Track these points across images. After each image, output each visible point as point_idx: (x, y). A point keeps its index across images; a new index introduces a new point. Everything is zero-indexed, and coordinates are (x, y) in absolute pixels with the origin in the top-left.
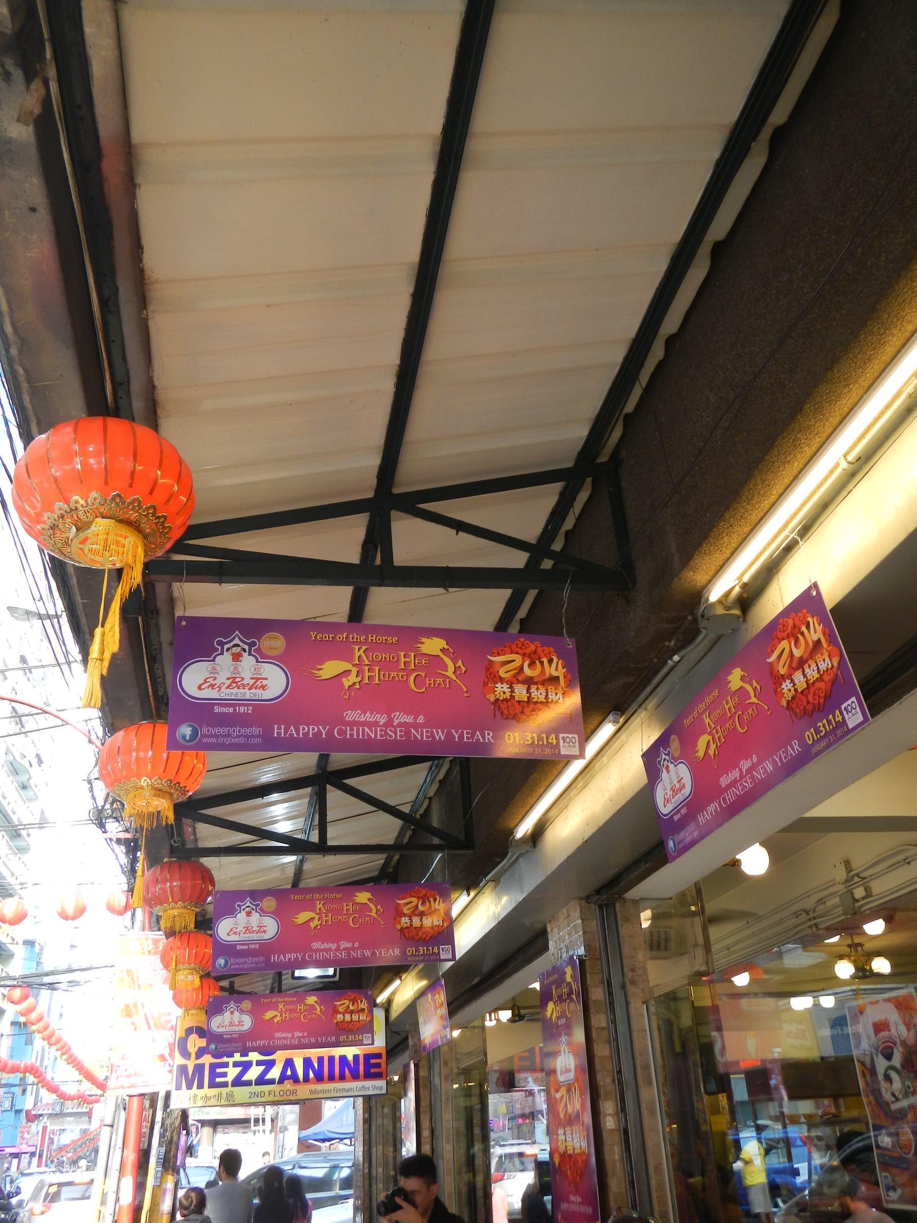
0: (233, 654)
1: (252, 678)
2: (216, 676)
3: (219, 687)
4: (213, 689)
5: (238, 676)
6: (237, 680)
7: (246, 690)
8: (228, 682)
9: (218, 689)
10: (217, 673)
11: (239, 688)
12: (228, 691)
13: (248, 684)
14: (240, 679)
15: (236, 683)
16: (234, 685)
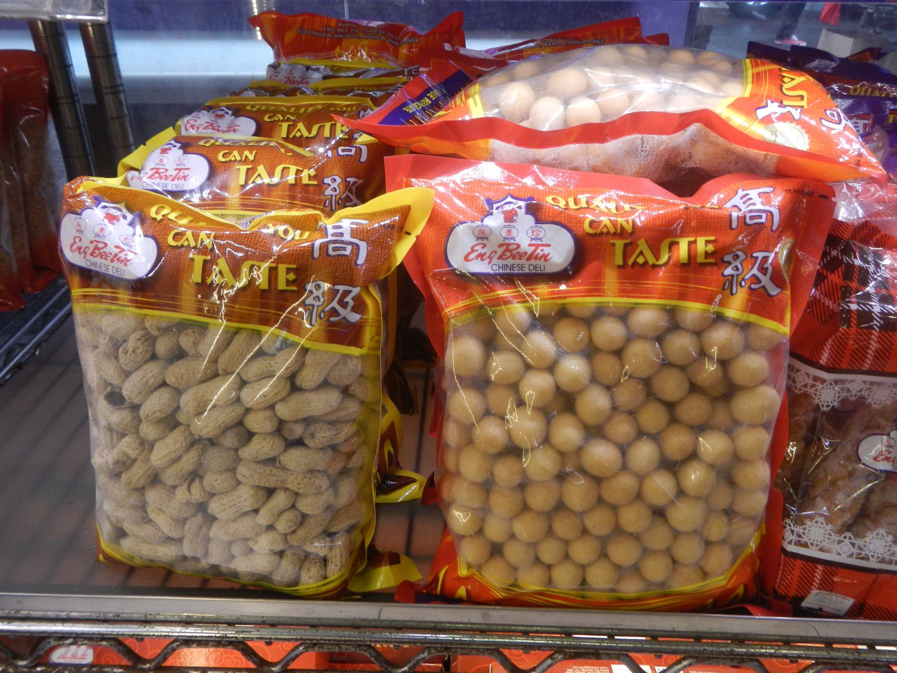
0: (505, 213)
1: (530, 245)
2: (485, 241)
3: (489, 257)
4: (482, 260)
5: (512, 241)
6: (511, 247)
7: (524, 261)
8: (500, 251)
9: (488, 260)
10: (487, 238)
11: (514, 258)
12: (501, 262)
13: (526, 253)
14: (515, 246)
15: (511, 251)
16: (508, 254)
